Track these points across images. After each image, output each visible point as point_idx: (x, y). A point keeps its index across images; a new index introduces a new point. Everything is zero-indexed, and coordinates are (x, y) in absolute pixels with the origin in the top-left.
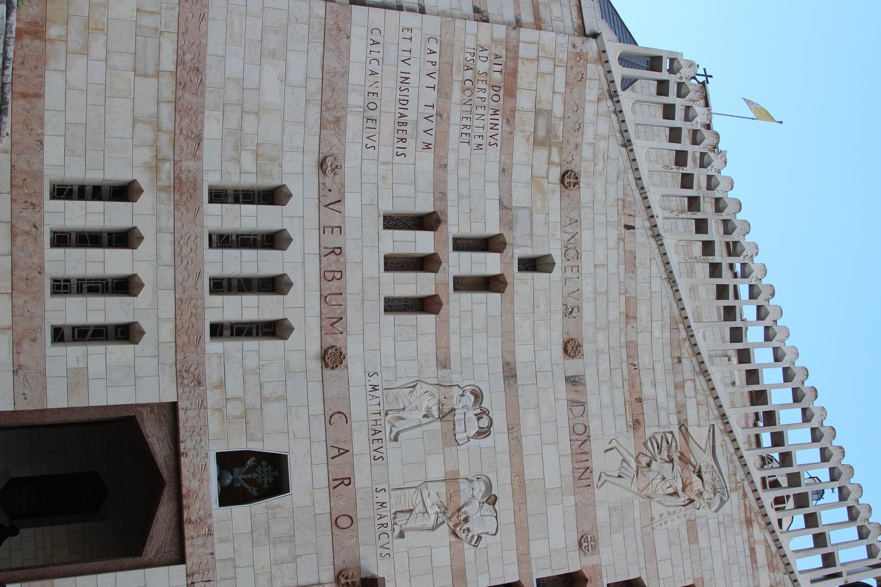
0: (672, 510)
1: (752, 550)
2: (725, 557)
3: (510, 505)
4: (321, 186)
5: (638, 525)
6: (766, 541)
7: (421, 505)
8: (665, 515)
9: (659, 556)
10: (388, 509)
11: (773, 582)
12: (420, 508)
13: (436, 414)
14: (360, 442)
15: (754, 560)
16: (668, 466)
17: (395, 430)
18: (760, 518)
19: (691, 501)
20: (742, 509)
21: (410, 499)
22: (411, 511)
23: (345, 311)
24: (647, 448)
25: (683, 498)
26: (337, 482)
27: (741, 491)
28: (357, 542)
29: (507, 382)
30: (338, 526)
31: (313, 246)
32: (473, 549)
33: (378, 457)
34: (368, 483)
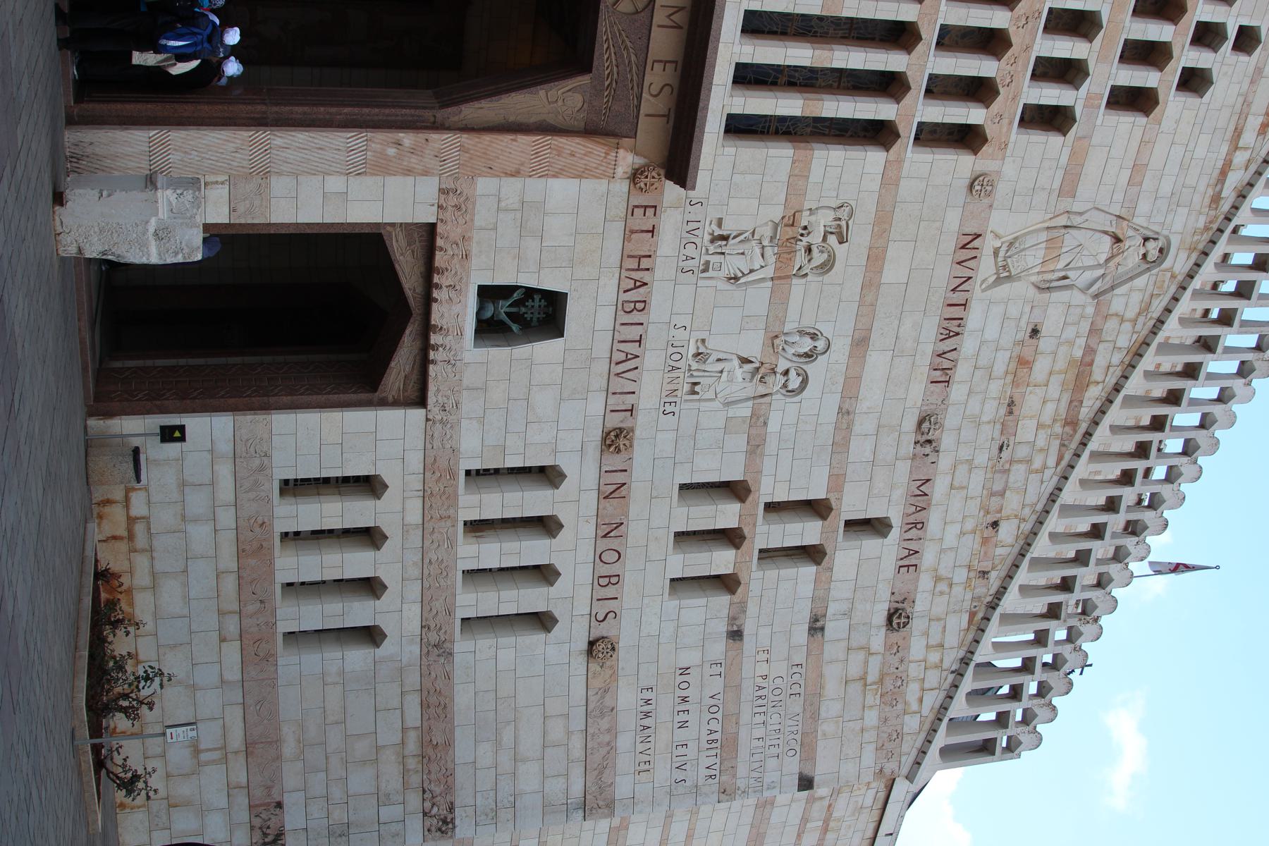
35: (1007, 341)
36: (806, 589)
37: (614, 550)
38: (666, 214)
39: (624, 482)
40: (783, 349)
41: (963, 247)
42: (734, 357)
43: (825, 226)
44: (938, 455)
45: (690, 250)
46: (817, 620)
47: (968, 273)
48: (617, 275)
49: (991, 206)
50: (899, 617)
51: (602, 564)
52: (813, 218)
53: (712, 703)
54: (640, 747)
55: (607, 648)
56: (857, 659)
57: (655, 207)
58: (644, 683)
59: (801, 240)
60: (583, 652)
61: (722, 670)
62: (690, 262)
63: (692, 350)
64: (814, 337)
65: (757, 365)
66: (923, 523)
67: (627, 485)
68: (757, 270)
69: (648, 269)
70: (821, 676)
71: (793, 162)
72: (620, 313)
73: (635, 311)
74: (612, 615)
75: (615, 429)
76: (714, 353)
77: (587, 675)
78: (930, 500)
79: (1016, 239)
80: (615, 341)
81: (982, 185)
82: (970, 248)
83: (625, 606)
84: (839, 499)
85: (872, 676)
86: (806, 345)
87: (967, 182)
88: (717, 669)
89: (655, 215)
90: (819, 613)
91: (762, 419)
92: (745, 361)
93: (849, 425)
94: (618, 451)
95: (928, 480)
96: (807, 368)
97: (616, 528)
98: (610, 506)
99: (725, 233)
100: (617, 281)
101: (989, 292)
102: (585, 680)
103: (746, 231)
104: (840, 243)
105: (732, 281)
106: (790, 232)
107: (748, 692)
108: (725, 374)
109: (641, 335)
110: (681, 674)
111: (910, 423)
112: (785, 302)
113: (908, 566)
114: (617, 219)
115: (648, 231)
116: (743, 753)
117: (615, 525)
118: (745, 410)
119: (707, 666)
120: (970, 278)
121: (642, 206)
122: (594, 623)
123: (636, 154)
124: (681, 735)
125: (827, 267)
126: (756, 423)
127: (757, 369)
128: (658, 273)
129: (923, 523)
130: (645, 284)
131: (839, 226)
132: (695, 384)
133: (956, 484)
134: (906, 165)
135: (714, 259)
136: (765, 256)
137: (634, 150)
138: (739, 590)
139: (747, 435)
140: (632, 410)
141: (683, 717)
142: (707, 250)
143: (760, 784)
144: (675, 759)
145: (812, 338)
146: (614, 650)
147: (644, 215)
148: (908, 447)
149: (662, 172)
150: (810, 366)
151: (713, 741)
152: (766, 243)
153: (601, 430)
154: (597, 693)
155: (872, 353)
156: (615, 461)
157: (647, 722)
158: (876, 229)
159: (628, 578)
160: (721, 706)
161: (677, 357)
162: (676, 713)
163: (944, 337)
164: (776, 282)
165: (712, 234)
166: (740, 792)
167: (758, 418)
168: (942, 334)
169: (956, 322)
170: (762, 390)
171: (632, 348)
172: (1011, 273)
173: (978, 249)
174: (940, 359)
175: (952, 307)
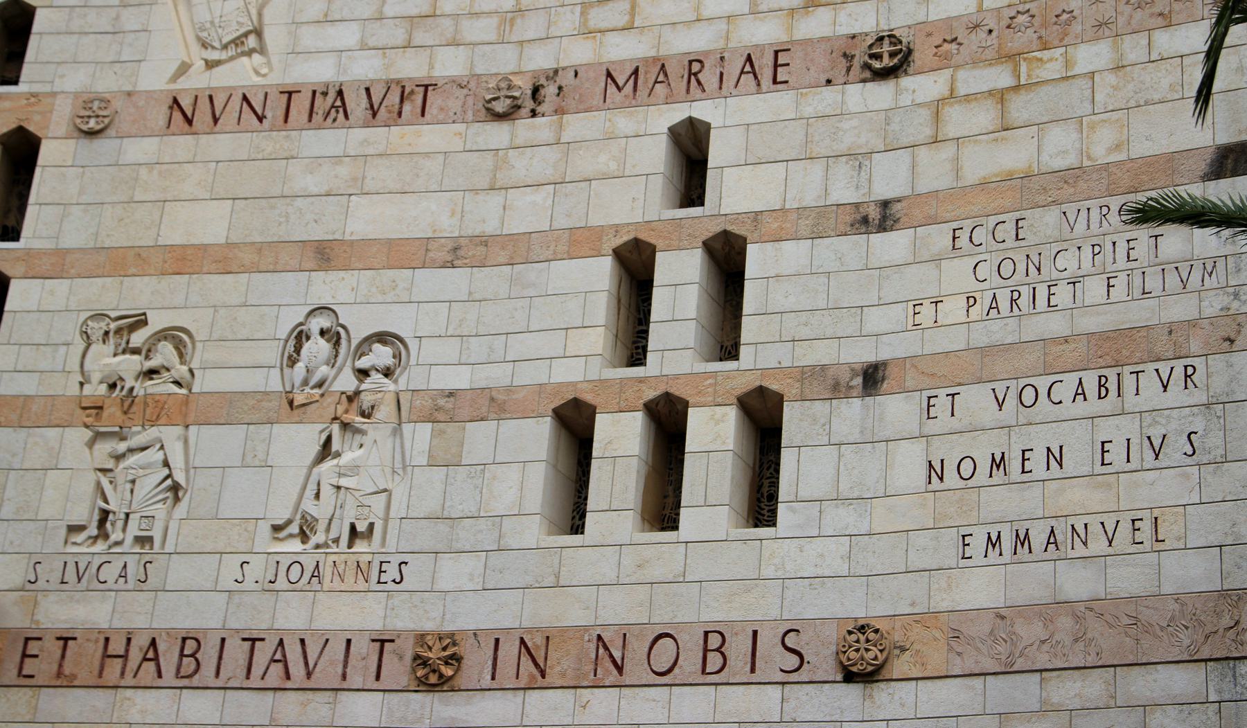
36: (793, 254)
37: (678, 648)
38: (42, 620)
39: (518, 642)
40: (320, 385)
41: (190, 122)
42: (316, 470)
43: (115, 355)
44: (563, 69)
45: (109, 573)
46: (865, 220)
47: (237, 99)
48: (129, 693)
49: (129, 94)
50: (878, 57)
51: (676, 670)
52: (96, 377)
53: (1015, 401)
54: (1098, 545)
55: (858, 641)
56: (958, 120)
57: (27, 639)
58: (950, 555)
59: (132, 389)
60: (868, 691)
61: (942, 393)
63: (295, 546)
64: (301, 337)
65: (336, 428)
66: (690, 62)
67: (524, 637)
68: (165, 454)
69: (129, 640)
70: (983, 184)
72: (196, 681)
73: (197, 656)
74: (791, 641)
75: (414, 671)
76: (303, 506)
77: (917, 679)
78: (645, 60)
79: (199, 38)
80: (246, 684)
81: (89, 117)
82: (194, 110)
83: (774, 613)
84: (617, 229)
85: (1001, 77)
86: (317, 348)
87: (85, 142)
88: (942, 403)
89: (40, 639)
90: (848, 219)
91: (441, 402)
92: (326, 450)
94: (455, 660)
95: (609, 75)
96: (358, 335)
97: (606, 648)
98: (561, 663)
99: (96, 517)
100: (140, 692)
101: (275, 59)
102: (929, 683)
103: (99, 485)
104: (144, 323)
105: (180, 494)
107: (1001, 331)
108: (343, 482)
109: (244, 640)
110: (941, 479)
111: (498, 134)
113: (776, 66)
114: (34, 702)
115: (65, 648)
116: (1139, 314)
117: (601, 650)
118: (420, 436)
119: (931, 427)
120: (245, 98)
121: (22, 662)
122: (803, 675)
124: (1079, 458)
125: (176, 337)
126: (446, 412)
127: (345, 426)
128: (140, 622)
129: (690, 62)
130: (154, 640)
131: (118, 331)
132: (353, 528)
133: (623, 21)
134: (37, 244)
135: (133, 530)
136: (143, 445)
138: (774, 387)
140: (383, 642)
141: (1037, 461)
142: (117, 543)
143: (1221, 264)
144: (1135, 464)
145: (308, 338)
146: (863, 627)
147: (36, 656)
148: (540, 128)
150: (352, 336)
151: (1100, 386)
152: (122, 447)
153: (414, 694)
154: (959, 654)
155: (348, 231)
156: (476, 663)
157: (1038, 538)
158: (132, 270)
159: (715, 612)
160: (1022, 382)
161: (296, 569)
162: (1026, 477)
163: (341, 115)
164: (190, 420)
165: (96, 538)
166: (1235, 305)
167: (439, 409)
168: (335, 120)
169: (319, 99)
170: (385, 412)
171: (264, 653)
172: (249, 32)
173: (196, 97)
174: (382, 113)
175: (291, 114)
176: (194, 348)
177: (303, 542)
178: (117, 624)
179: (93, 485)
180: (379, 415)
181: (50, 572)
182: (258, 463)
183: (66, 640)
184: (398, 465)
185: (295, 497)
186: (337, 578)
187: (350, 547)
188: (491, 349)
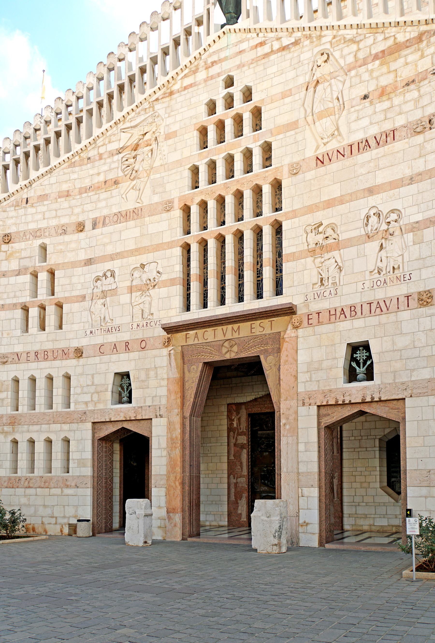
0: (159, 152)
1: (185, 88)
2: (186, 109)
3: (145, 256)
4: (12, 363)
5: (163, 174)
6: (182, 78)
7: (140, 305)
8: (161, 156)
9: (179, 158)
10: (140, 322)
11: (204, 68)
12: (141, 306)
13: (104, 300)
14: (112, 338)
15: (191, 86)
16: (138, 157)
17: (109, 321)
18: (170, 85)
19: (156, 139)
20: (164, 100)
21: (137, 311)
22: (142, 310)
23: (60, 349)
24: (128, 174)
25: (154, 146)
26: (127, 348)
27: (154, 103)
28: (152, 337)
29: (93, 263)
30: (145, 347)
31: (34, 365)
32: (163, 275)
33: (118, 329)
34: (129, 333)
35: (369, 110)
42: (380, 254)
45: (326, 294)
62: (332, 292)
69: (336, 310)
71: (288, 261)
91: (414, 225)
93: (419, 175)
99: (320, 280)
103: (318, 271)
105: (342, 269)
106: (318, 250)
108: (388, 255)
112: (350, 239)
123: (287, 329)
130: (342, 309)
137: (285, 331)
139: (424, 230)
149: (294, 316)
161: (379, 282)
167: (414, 228)
176: (337, 228)
177: (379, 274)
178: (331, 307)
179: (317, 272)
180: (396, 234)
181: (310, 297)
182: (362, 255)
183: (319, 313)
184: (404, 247)
185: (375, 262)
186: (391, 282)
187: (393, 273)
188: (428, 206)
